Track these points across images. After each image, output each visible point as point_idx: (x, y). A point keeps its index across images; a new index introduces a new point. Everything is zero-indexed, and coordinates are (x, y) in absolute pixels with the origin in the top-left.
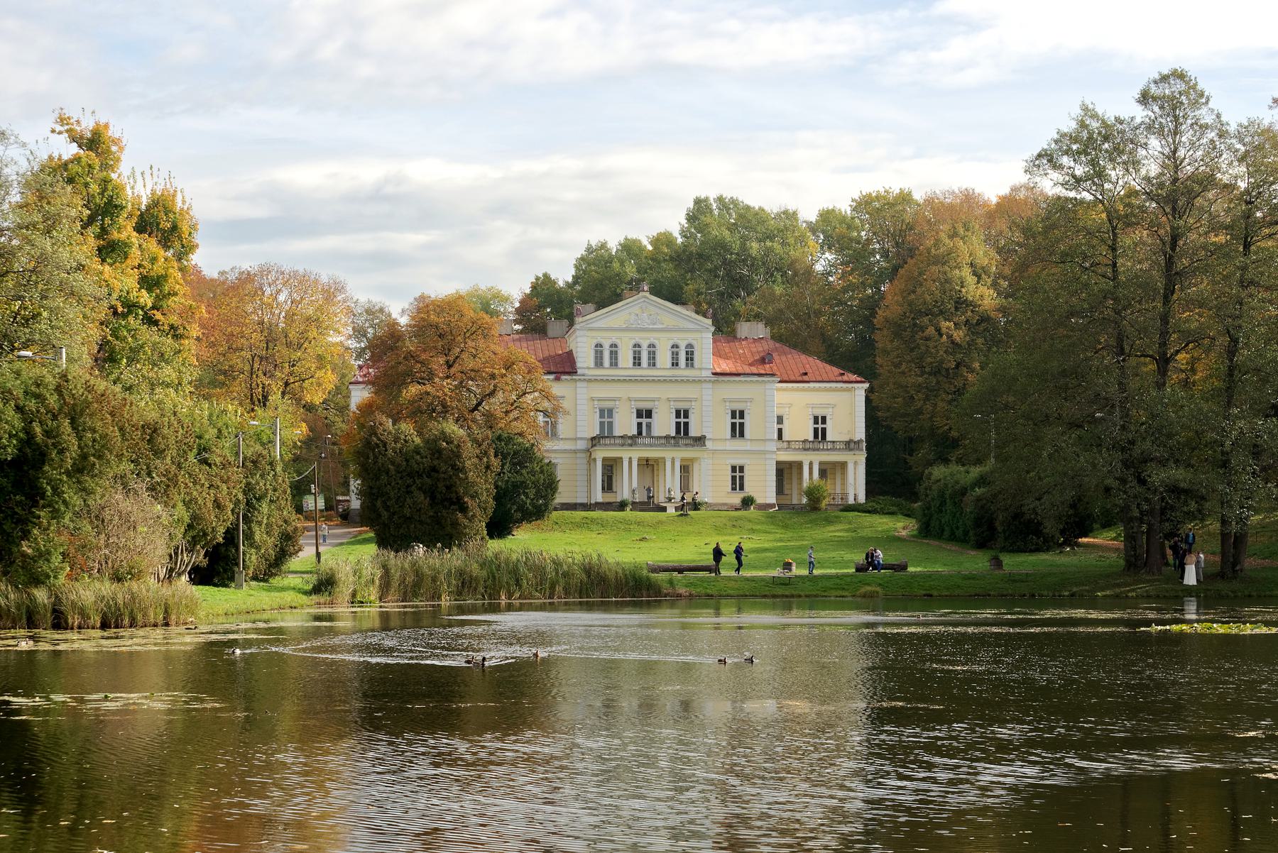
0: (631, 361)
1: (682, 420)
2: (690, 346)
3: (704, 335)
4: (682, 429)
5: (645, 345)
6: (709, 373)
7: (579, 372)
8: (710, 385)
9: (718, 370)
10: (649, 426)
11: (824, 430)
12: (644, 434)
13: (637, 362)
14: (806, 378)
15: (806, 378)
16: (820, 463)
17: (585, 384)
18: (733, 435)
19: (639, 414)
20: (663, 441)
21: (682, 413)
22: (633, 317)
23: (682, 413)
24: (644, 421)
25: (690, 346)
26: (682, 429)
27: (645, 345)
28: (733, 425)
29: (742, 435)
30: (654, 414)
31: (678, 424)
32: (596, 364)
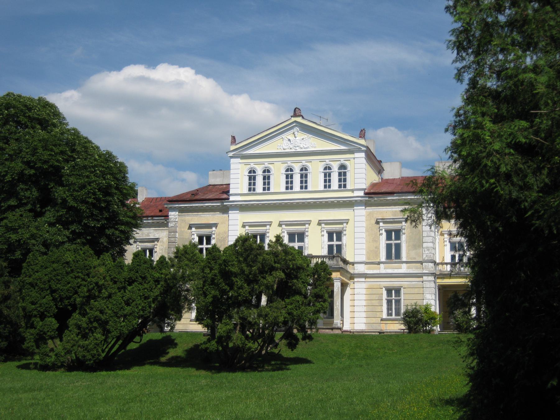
0: (284, 185)
1: (335, 243)
2: (343, 167)
3: (357, 155)
5: (297, 169)
6: (362, 193)
7: (232, 198)
13: (289, 186)
18: (389, 256)
21: (335, 235)
22: (286, 141)
23: (335, 235)
25: (343, 167)
27: (297, 169)
28: (389, 247)
30: (306, 240)
31: (330, 247)
32: (250, 190)
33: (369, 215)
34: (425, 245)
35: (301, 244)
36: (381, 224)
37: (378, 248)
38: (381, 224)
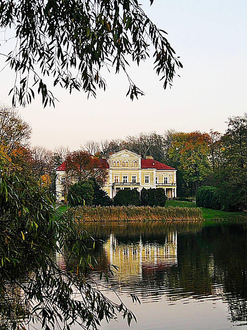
4: (134, 181)
6: (140, 168)
8: (140, 170)
9: (143, 167)
10: (126, 180)
11: (167, 181)
12: (125, 182)
14: (162, 169)
15: (162, 169)
16: (166, 189)
17: (111, 170)
18: (146, 182)
19: (124, 177)
20: (130, 184)
24: (125, 179)
26: (134, 181)
27: (125, 161)
28: (146, 180)
29: (148, 182)
33: (142, 173)
34: (154, 180)
35: (126, 179)
36: (145, 175)
37: (144, 180)
38: (145, 175)
